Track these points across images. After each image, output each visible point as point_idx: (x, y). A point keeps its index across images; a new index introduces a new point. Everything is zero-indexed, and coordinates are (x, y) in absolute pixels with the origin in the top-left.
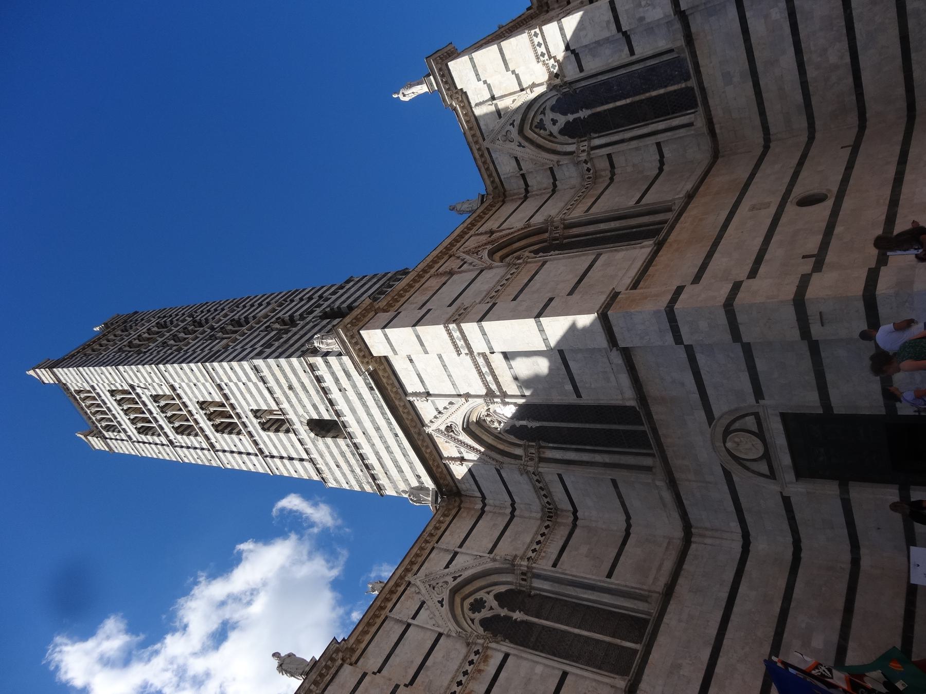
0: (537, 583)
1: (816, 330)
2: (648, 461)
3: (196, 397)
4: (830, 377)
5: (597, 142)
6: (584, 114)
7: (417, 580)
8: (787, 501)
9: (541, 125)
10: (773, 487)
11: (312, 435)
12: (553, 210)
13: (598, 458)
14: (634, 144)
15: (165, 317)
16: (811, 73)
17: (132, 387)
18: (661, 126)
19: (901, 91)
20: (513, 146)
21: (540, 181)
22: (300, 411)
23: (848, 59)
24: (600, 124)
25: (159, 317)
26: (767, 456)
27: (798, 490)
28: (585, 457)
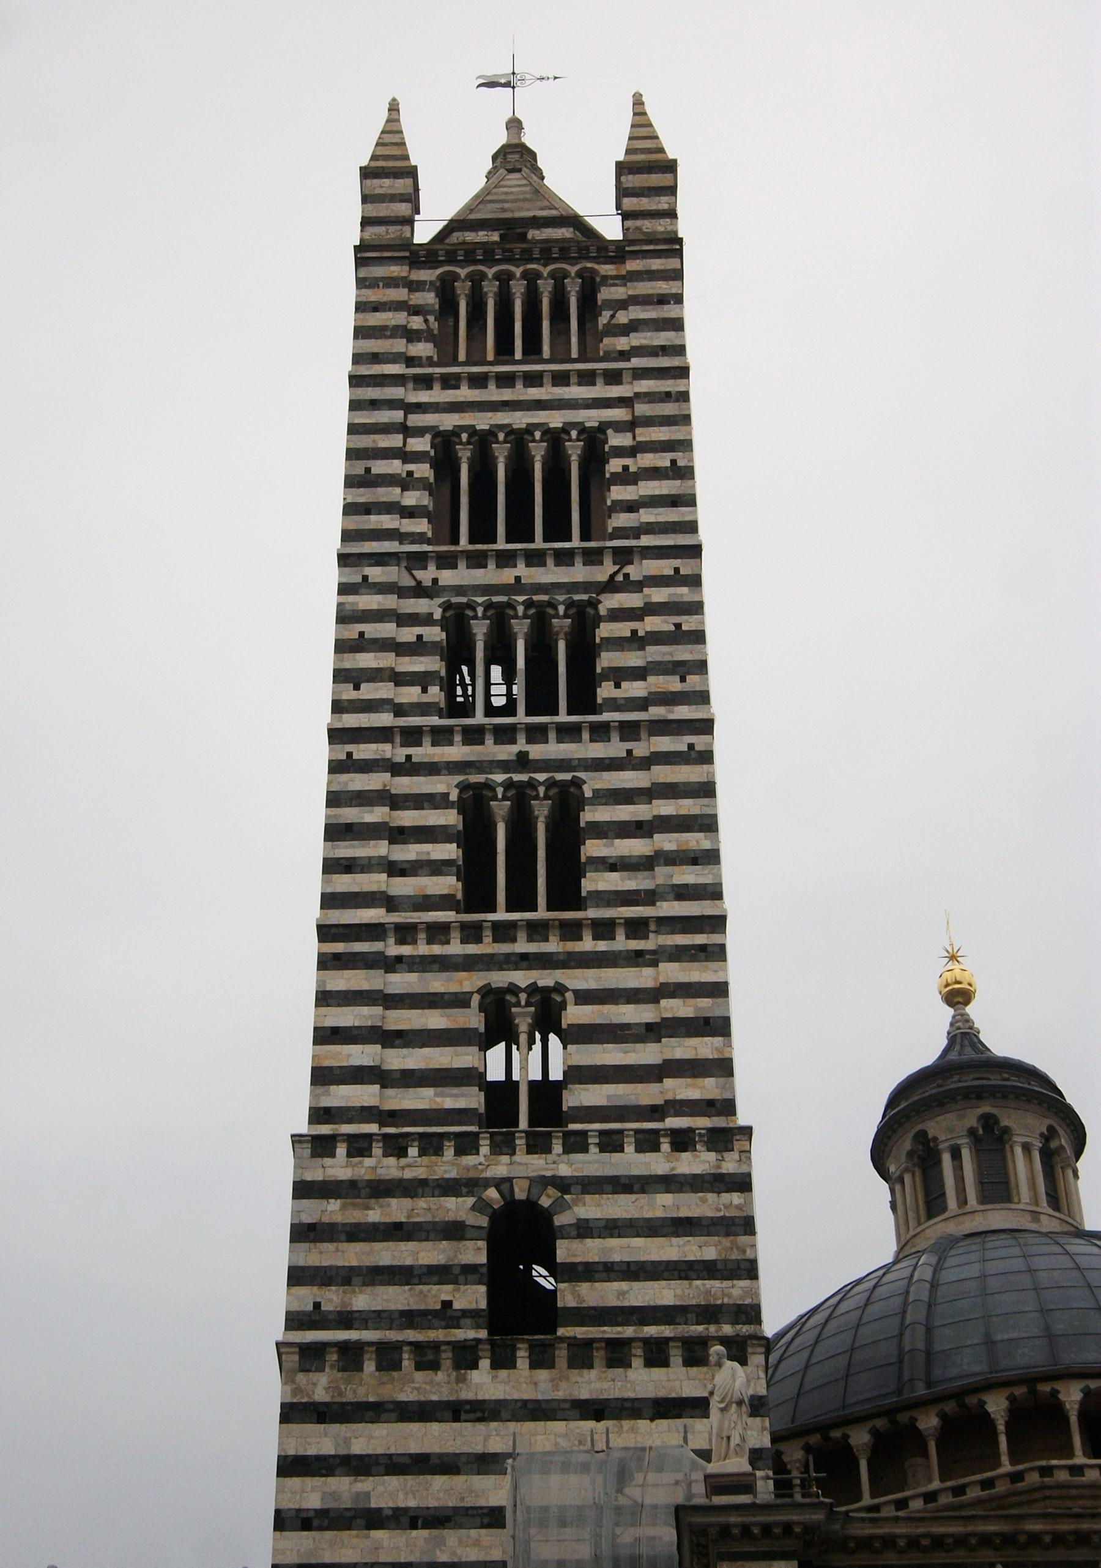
17: (623, 556)
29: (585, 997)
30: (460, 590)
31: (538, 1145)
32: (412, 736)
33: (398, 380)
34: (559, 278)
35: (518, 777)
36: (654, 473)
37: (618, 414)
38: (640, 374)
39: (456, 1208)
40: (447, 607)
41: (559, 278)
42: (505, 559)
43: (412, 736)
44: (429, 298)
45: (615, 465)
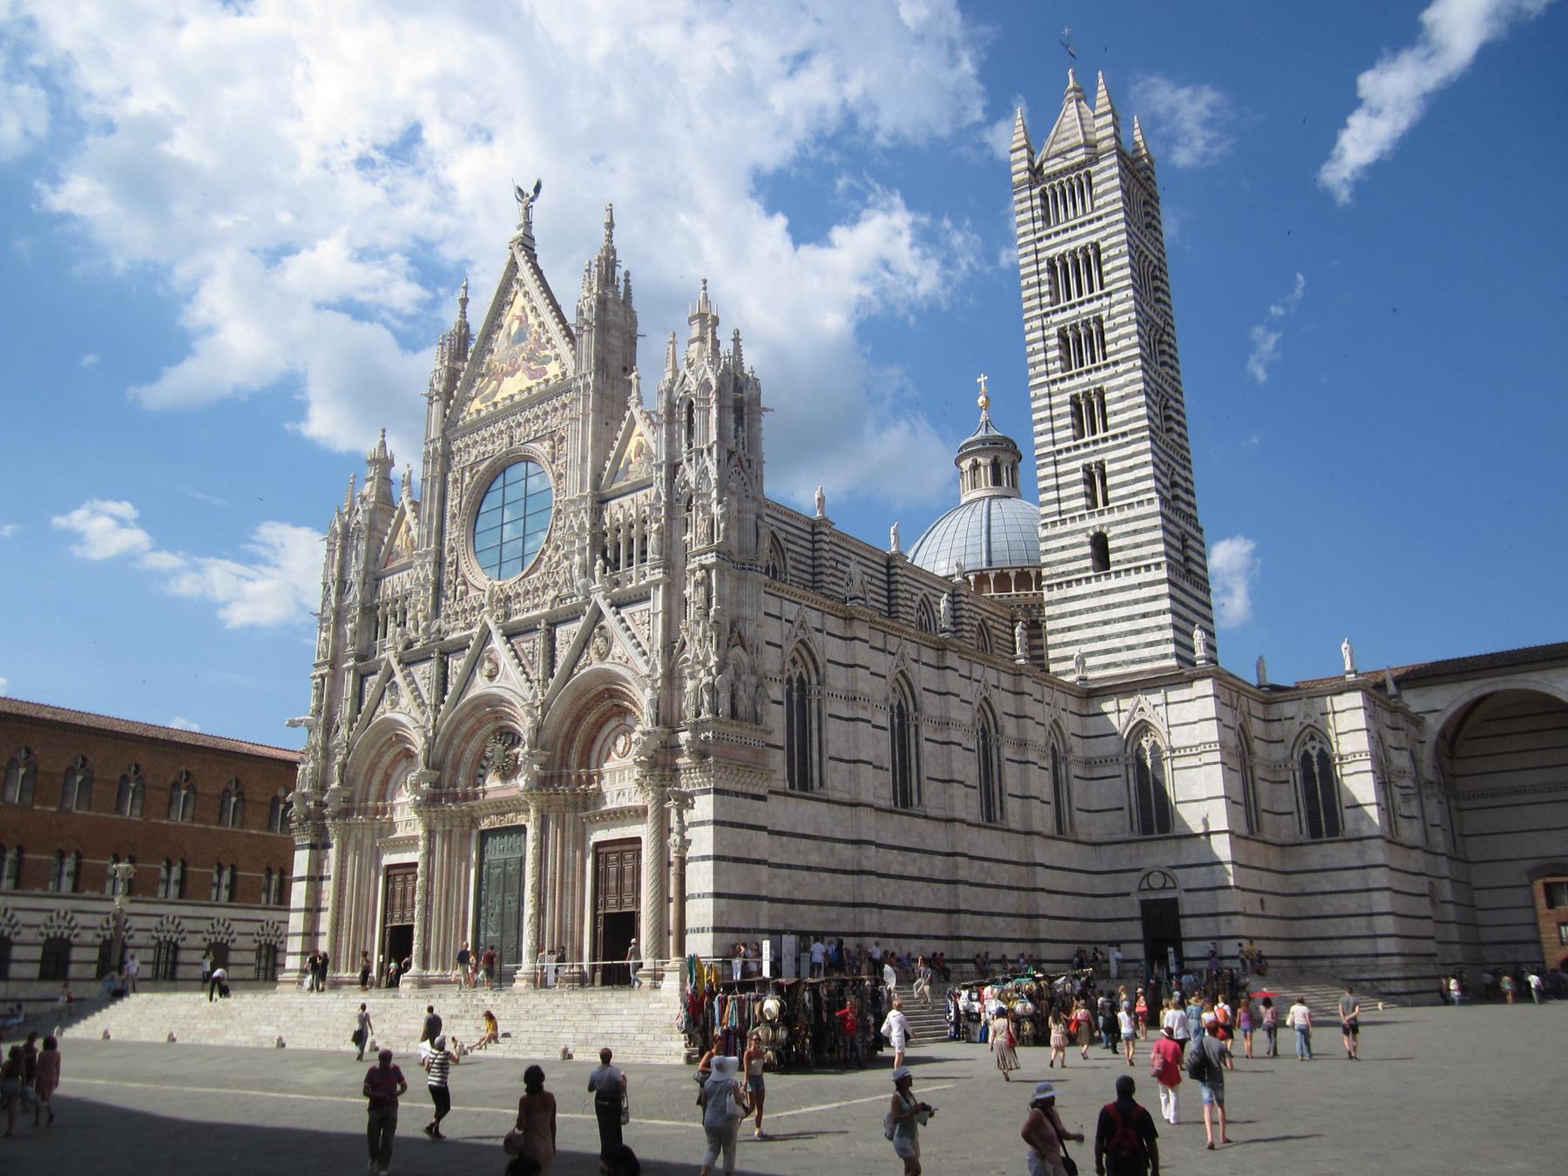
0: (1063, 767)
1: (1223, 918)
2: (1136, 828)
3: (1111, 390)
4: (1199, 919)
5: (1297, 774)
6: (1316, 769)
7: (1057, 694)
8: (1128, 894)
9: (1312, 738)
10: (1133, 888)
11: (1091, 533)
12: (1258, 746)
13: (1133, 801)
14: (1294, 798)
15: (1160, 270)
16: (1320, 898)
17: (1109, 294)
18: (1303, 815)
19: (1305, 935)
20: (1301, 719)
21: (1276, 731)
22: (1114, 531)
23: (1324, 914)
24: (1308, 777)
25: (1159, 259)
26: (1151, 889)
27: (1135, 899)
28: (1132, 792)
29: (1112, 461)
30: (1062, 322)
31: (1101, 513)
32: (1054, 382)
33: (1033, 242)
34: (1078, 177)
35: (1086, 389)
36: (1115, 257)
37: (1103, 234)
38: (1107, 215)
39: (1082, 538)
40: (1059, 330)
41: (1078, 177)
42: (1072, 307)
43: (1054, 382)
44: (1037, 202)
45: (1103, 256)
